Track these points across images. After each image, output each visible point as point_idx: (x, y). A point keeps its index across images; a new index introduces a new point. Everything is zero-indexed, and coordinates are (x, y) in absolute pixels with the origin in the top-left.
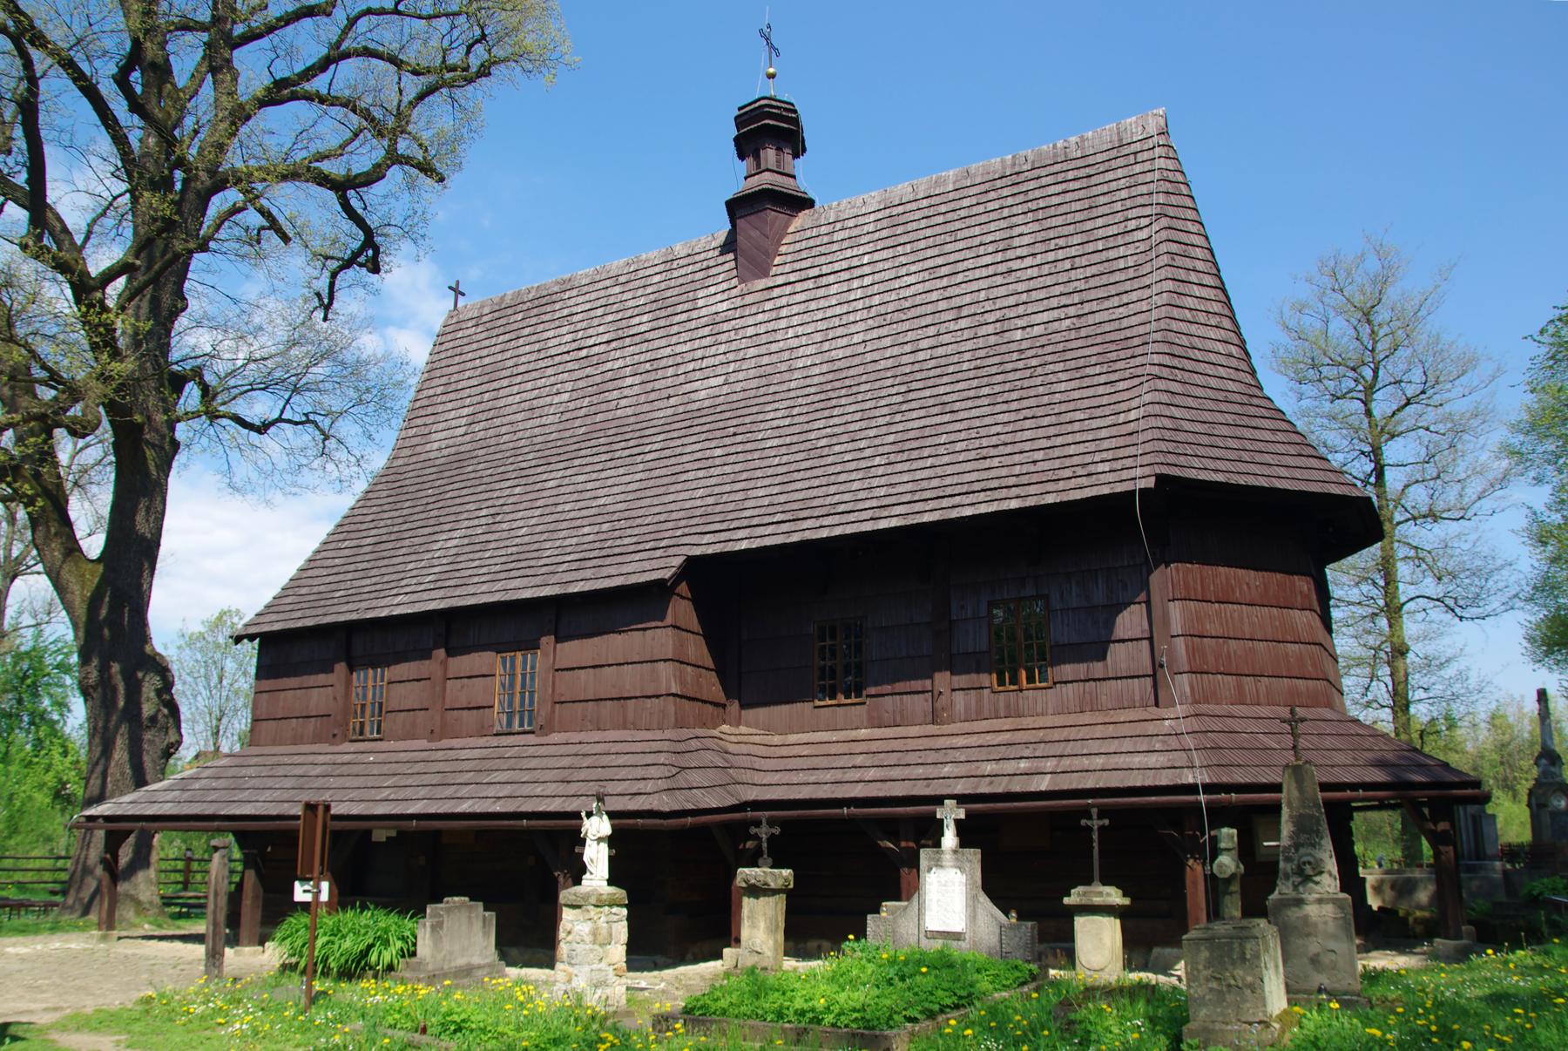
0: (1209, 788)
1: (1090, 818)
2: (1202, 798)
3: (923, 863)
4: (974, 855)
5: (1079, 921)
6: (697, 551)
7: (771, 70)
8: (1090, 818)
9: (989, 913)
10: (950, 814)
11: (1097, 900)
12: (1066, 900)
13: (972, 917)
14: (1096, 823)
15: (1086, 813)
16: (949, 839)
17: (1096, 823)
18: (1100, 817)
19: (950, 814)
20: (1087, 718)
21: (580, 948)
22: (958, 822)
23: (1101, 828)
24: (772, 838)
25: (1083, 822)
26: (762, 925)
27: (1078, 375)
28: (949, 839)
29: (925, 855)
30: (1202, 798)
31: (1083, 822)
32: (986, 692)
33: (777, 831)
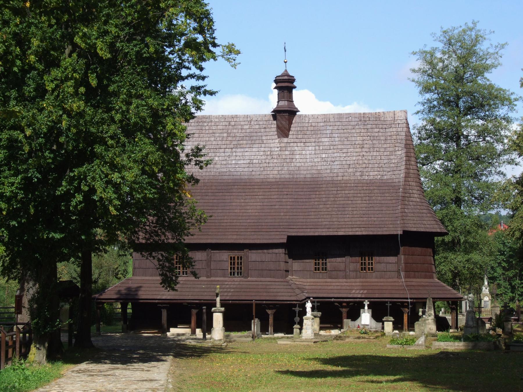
0: (411, 299)
1: (388, 303)
2: (409, 300)
3: (361, 312)
4: (370, 310)
5: (385, 323)
6: (290, 234)
7: (286, 61)
8: (388, 303)
9: (374, 321)
10: (366, 303)
11: (389, 319)
12: (383, 319)
13: (371, 322)
14: (389, 305)
15: (387, 302)
16: (366, 308)
17: (389, 305)
18: (390, 303)
19: (366, 303)
20: (382, 280)
21: (308, 327)
22: (368, 304)
23: (390, 306)
24: (318, 306)
25: (386, 304)
26: (316, 324)
27: (383, 195)
28: (366, 308)
29: (362, 310)
30: (409, 300)
31: (386, 304)
32: (358, 272)
33: (319, 304)
